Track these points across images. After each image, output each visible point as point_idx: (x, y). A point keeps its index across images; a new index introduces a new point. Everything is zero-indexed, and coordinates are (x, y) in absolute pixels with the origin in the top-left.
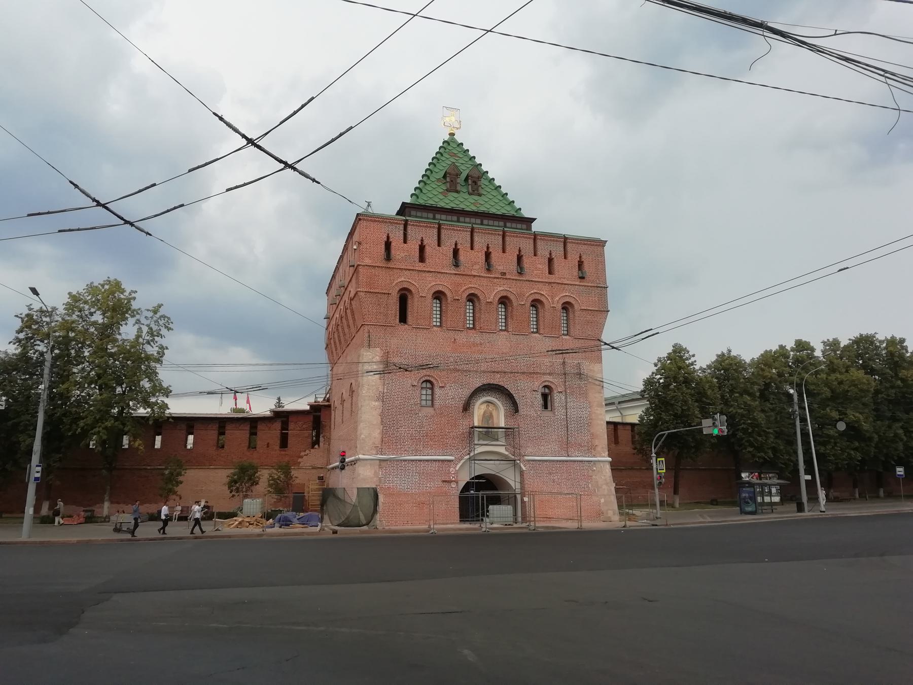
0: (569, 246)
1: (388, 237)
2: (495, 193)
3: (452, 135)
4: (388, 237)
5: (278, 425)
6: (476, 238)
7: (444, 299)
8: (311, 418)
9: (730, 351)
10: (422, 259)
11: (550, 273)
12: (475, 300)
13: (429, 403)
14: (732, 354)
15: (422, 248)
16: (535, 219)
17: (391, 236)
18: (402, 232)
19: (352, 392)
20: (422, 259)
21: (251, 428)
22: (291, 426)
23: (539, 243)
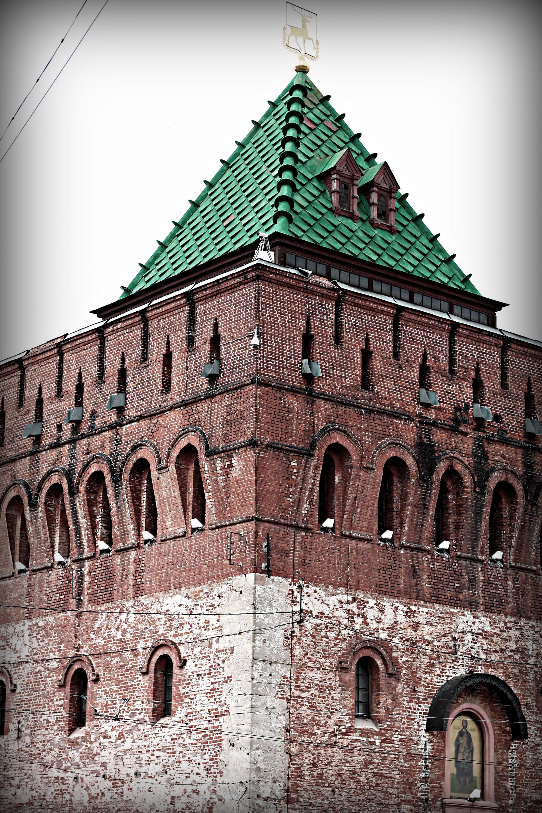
2: (411, 227)
3: (303, 70)
4: (308, 324)
6: (458, 348)
10: (366, 382)
15: (367, 354)
20: (366, 382)
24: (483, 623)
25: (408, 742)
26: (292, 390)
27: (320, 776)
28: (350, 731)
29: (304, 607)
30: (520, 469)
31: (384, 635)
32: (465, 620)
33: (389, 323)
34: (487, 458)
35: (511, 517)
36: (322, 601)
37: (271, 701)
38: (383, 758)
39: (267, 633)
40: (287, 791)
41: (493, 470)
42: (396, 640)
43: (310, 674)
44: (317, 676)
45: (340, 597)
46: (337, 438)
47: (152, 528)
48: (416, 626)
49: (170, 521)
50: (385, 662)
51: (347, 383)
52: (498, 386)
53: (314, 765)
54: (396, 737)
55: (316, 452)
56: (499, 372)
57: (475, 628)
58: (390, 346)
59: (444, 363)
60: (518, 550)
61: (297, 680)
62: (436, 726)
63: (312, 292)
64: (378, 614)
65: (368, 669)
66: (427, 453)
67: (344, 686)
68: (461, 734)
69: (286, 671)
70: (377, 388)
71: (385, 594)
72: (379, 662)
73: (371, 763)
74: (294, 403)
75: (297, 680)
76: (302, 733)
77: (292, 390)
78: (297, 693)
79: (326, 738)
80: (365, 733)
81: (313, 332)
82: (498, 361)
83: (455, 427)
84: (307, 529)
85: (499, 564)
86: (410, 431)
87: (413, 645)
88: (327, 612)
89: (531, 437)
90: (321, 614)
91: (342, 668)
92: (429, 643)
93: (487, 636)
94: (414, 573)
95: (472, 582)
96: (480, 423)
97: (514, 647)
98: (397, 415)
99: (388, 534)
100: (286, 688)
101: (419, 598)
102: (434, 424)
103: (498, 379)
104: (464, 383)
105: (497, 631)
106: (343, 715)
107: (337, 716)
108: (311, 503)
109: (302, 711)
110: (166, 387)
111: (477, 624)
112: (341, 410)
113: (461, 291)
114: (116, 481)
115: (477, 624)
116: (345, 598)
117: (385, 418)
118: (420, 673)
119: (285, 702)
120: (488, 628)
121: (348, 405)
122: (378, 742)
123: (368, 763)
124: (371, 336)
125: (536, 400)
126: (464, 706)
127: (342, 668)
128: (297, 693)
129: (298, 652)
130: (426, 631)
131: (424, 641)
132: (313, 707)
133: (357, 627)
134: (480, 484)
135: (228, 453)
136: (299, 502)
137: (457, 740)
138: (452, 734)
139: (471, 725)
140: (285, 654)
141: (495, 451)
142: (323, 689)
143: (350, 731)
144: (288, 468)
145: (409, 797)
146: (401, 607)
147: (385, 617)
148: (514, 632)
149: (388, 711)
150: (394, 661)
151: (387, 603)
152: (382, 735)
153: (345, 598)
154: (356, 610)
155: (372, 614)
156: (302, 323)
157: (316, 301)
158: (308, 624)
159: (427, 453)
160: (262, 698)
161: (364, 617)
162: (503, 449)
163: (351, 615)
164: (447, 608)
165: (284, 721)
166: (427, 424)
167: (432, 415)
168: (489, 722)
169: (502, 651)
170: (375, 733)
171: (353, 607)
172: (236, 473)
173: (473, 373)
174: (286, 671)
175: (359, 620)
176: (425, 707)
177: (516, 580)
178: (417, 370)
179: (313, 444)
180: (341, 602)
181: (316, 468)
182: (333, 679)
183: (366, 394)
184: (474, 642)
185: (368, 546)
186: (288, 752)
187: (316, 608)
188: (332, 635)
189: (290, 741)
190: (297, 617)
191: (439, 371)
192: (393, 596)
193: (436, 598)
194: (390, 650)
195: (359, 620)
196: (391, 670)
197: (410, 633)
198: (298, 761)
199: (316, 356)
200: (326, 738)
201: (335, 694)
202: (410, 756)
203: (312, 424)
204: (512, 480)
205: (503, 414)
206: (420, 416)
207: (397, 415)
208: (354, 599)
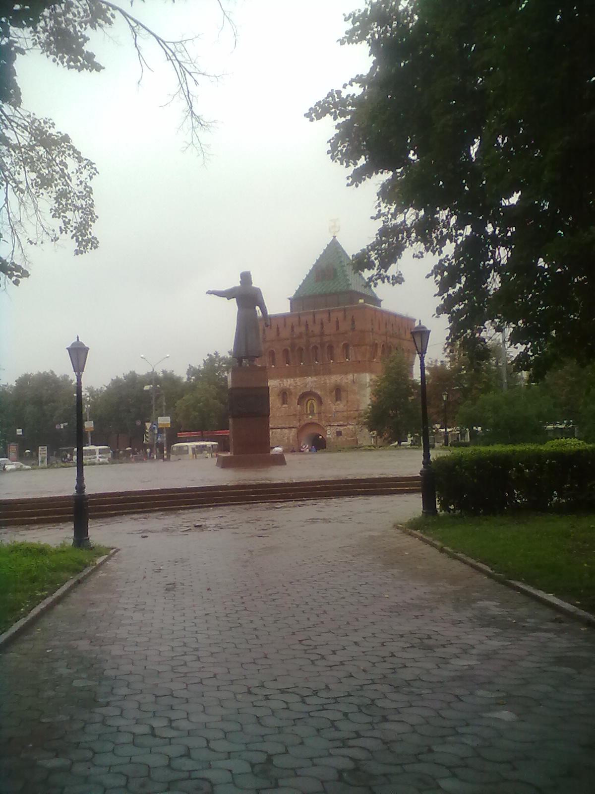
11: (338, 328)
24: (315, 379)
31: (288, 387)
32: (309, 379)
46: (271, 349)
91: (279, 395)
93: (315, 381)
127: (279, 395)
130: (299, 384)
159: (293, 346)
163: (280, 384)
175: (282, 385)
192: (291, 377)
193: (301, 376)
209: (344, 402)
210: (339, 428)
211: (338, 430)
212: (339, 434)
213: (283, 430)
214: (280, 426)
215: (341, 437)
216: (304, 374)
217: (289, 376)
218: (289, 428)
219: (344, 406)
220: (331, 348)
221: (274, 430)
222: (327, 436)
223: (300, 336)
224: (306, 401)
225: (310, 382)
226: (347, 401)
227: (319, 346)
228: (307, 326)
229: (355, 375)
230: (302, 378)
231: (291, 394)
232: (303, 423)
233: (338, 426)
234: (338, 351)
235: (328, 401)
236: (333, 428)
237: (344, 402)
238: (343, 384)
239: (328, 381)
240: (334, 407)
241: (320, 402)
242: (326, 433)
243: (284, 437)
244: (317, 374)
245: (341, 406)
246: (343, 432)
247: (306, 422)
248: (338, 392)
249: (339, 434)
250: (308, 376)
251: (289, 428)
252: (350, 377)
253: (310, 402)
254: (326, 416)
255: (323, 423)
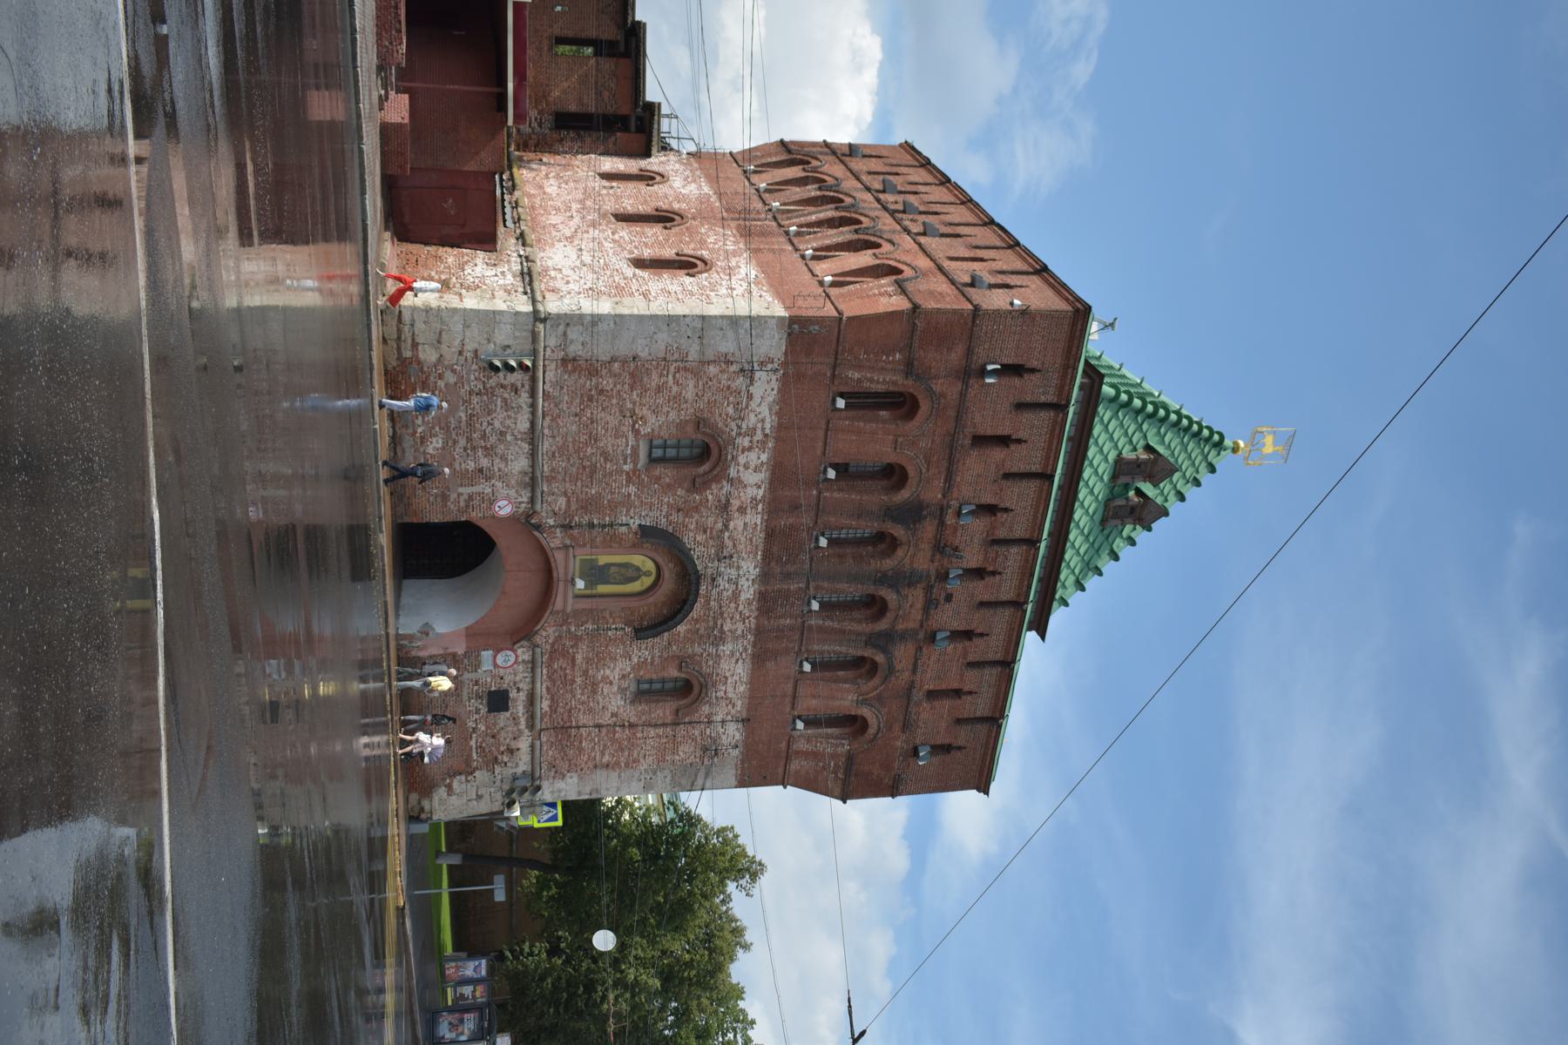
0: (982, 729)
1: (1033, 371)
4: (1033, 371)
5: (608, 32)
6: (1014, 550)
7: (884, 483)
8: (625, 110)
9: (746, 947)
10: (980, 441)
11: (932, 695)
12: (882, 546)
13: (658, 453)
14: (740, 952)
16: (1043, 638)
17: (1035, 378)
18: (1043, 399)
19: (686, 265)
20: (980, 441)
21: (612, 44)
22: (607, 64)
23: (996, 671)
24: (748, 591)
25: (627, 502)
26: (969, 352)
27: (590, 399)
28: (636, 433)
29: (757, 375)
30: (900, 627)
31: (732, 472)
32: (749, 568)
33: (1036, 468)
34: (910, 585)
35: (852, 620)
36: (763, 399)
37: (663, 337)
38: (611, 474)
39: (730, 334)
40: (574, 359)
41: (898, 592)
42: (727, 487)
43: (691, 384)
44: (690, 394)
45: (768, 420)
47: (814, 258)
48: (742, 510)
49: (826, 270)
50: (705, 473)
51: (978, 419)
52: (979, 598)
53: (601, 392)
54: (632, 489)
55: (910, 382)
56: (993, 599)
57: (743, 581)
58: (1015, 470)
59: (1002, 533)
60: (821, 629)
61: (685, 369)
62: (648, 534)
63: (1064, 377)
64: (752, 465)
65: (699, 454)
66: (912, 514)
67: (681, 426)
68: (638, 569)
69: (693, 355)
70: (974, 453)
71: (773, 473)
72: (706, 467)
73: (606, 460)
74: (956, 356)
75: (685, 369)
76: (632, 375)
77: (969, 352)
78: (672, 369)
79: (629, 405)
80: (635, 450)
81: (1026, 376)
82: (1004, 597)
83: (940, 547)
84: (833, 376)
85: (806, 609)
86: (933, 494)
87: (724, 507)
88: (753, 404)
89: (932, 638)
90: (750, 397)
92: (726, 526)
93: (735, 596)
94: (795, 507)
95: (788, 576)
96: (943, 577)
97: (726, 629)
98: (949, 478)
99: (831, 474)
100: (676, 356)
101: (770, 513)
102: (942, 523)
103: (986, 598)
104: (981, 557)
105: (741, 608)
106: (652, 424)
107: (652, 419)
108: (859, 381)
109: (655, 376)
110: (952, 259)
111: (747, 584)
112: (952, 413)
113: (1053, 598)
114: (856, 231)
115: (747, 584)
116: (768, 426)
117: (945, 464)
118: (696, 516)
119: (662, 355)
120: (743, 597)
121: (958, 418)
122: (626, 468)
123: (605, 455)
124: (1024, 446)
125: (967, 643)
126: (666, 574)
128: (672, 369)
129: (713, 370)
130: (737, 523)
131: (728, 520)
132: (659, 389)
133: (739, 440)
134: (882, 579)
135: (904, 292)
136: (859, 367)
137: (632, 565)
138: (638, 560)
139: (647, 581)
140: (710, 355)
141: (916, 596)
142: (678, 399)
143: (636, 433)
144: (892, 351)
145: (573, 507)
146: (761, 492)
147: (751, 472)
148: (740, 627)
149: (658, 479)
150: (706, 485)
151: (762, 476)
152: (634, 471)
153: (768, 426)
154: (756, 438)
155: (753, 457)
156: (1035, 364)
157: (1055, 380)
158: (740, 382)
159: (912, 514)
160: (665, 328)
161: (750, 449)
162: (919, 605)
163: (751, 432)
164: (761, 547)
165: (643, 354)
166: (942, 510)
167: (950, 519)
168: (651, 600)
169: (722, 614)
170: (635, 462)
171: (759, 436)
172: (884, 300)
173: (991, 569)
174: (693, 355)
175: (746, 442)
176: (663, 522)
177: (791, 628)
178: (992, 501)
179: (918, 378)
180: (763, 421)
181: (895, 383)
182: (688, 412)
183: (967, 442)
184: (730, 580)
185: (819, 452)
186: (613, 359)
187: (757, 390)
188: (731, 410)
189: (624, 362)
190: (746, 367)
191: (993, 528)
192: (772, 482)
193: (771, 534)
194: (717, 479)
195: (746, 442)
196: (698, 480)
197: (735, 503)
198: (604, 372)
199: (1006, 380)
200: (629, 405)
201: (673, 415)
202: (613, 506)
203: (937, 377)
204: (890, 616)
205: (953, 605)
206: (949, 507)
207: (949, 478)
208: (766, 435)
209: (630, 713)
210: (522, 696)
211: (513, 694)
212: (498, 701)
213: (526, 447)
214: (544, 424)
215: (484, 710)
216: (779, 546)
217: (779, 475)
218: (533, 479)
219: (613, 715)
220: (861, 666)
221: (524, 397)
222: (487, 655)
223: (941, 547)
224: (660, 560)
225: (739, 579)
226: (631, 726)
227: (883, 625)
228: (979, 573)
229: (736, 752)
230: (760, 537)
231: (697, 485)
232: (555, 540)
233: (531, 699)
234: (846, 697)
235: (645, 651)
236: (522, 674)
237: (630, 713)
238: (706, 709)
239: (727, 648)
240: (614, 675)
241: (645, 630)
242: (498, 651)
243: (489, 451)
244: (767, 602)
245: (614, 703)
246: (504, 716)
247: (559, 557)
248: (684, 691)
249: (498, 701)
250: (768, 557)
251: (533, 479)
252: (733, 733)
253: (650, 566)
254: (577, 639)
255: (547, 633)
